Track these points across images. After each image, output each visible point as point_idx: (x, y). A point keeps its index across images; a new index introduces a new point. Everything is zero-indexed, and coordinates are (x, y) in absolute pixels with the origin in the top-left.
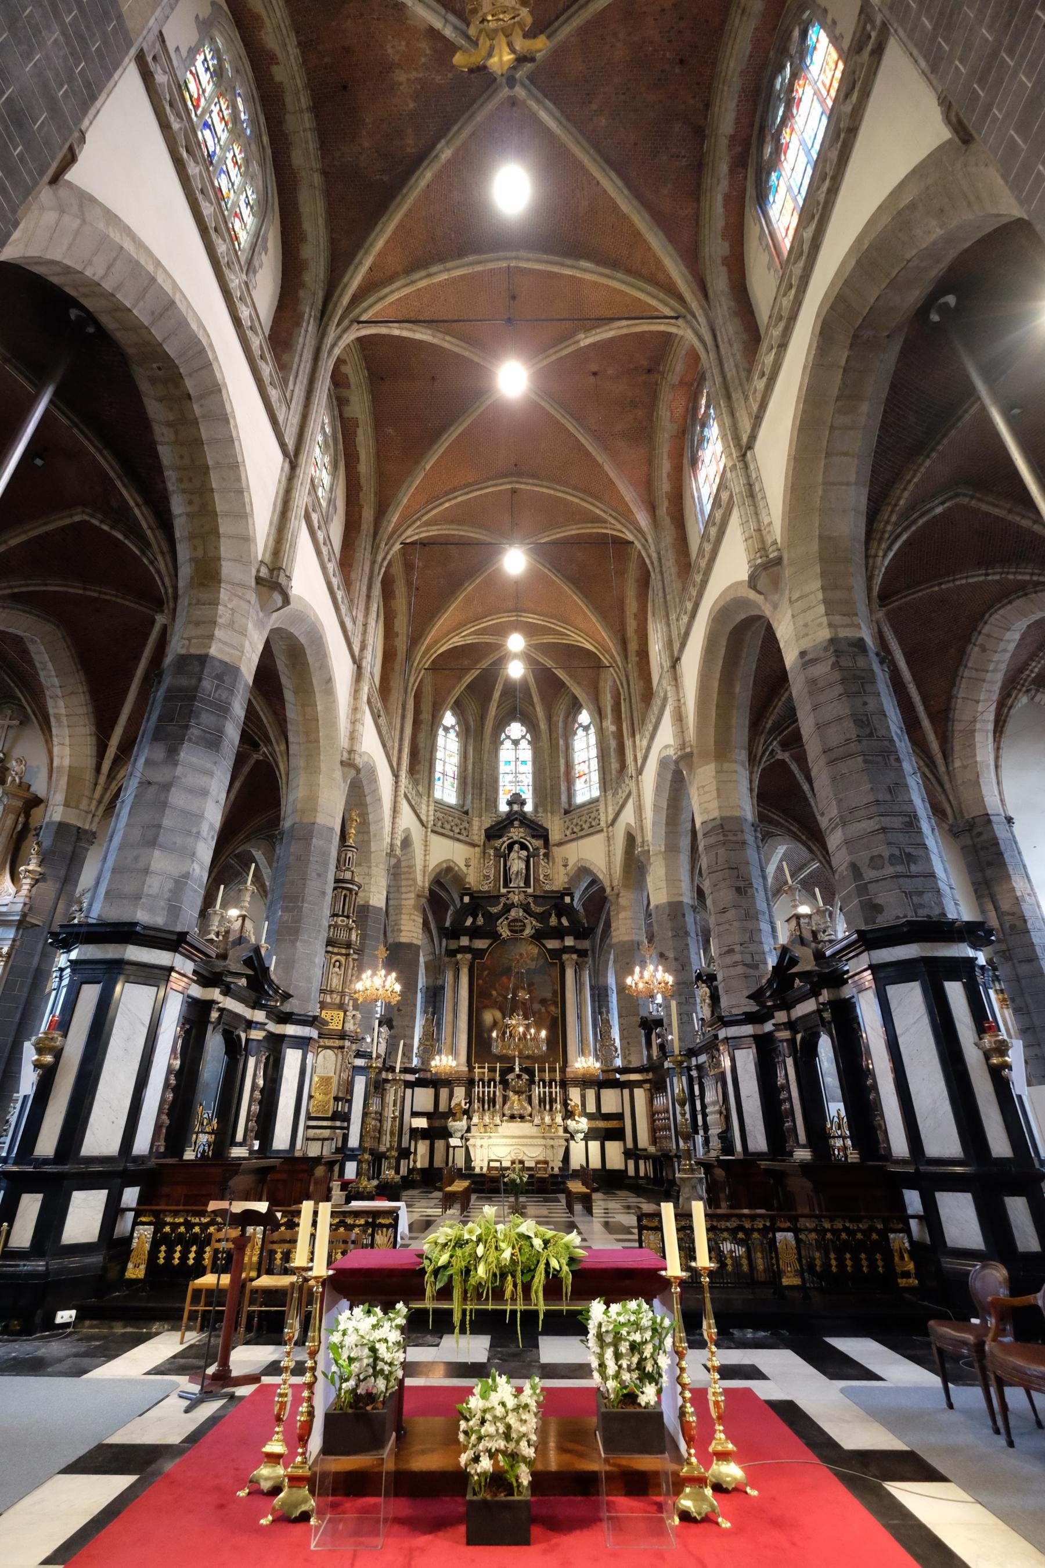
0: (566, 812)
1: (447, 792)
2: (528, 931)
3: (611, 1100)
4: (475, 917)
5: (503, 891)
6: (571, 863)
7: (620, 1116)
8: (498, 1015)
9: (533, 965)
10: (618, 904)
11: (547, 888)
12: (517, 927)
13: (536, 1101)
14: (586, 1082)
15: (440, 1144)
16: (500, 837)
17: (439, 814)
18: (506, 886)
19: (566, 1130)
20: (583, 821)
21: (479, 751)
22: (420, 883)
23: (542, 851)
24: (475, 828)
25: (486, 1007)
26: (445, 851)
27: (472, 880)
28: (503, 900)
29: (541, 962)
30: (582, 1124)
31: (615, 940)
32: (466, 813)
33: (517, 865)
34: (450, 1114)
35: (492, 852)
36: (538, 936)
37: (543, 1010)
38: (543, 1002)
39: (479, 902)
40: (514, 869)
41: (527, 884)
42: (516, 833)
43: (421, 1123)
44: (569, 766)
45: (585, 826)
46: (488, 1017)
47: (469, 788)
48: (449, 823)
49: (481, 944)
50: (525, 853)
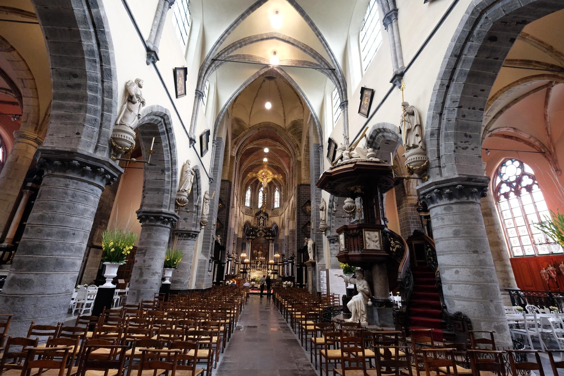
1: (248, 204)
3: (276, 268)
7: (277, 270)
12: (261, 234)
14: (271, 264)
15: (245, 274)
20: (276, 212)
21: (255, 194)
26: (249, 218)
30: (271, 271)
33: (261, 222)
34: (247, 269)
36: (265, 236)
39: (254, 229)
42: (262, 215)
43: (242, 270)
44: (274, 199)
46: (254, 252)
48: (248, 212)
49: (254, 237)
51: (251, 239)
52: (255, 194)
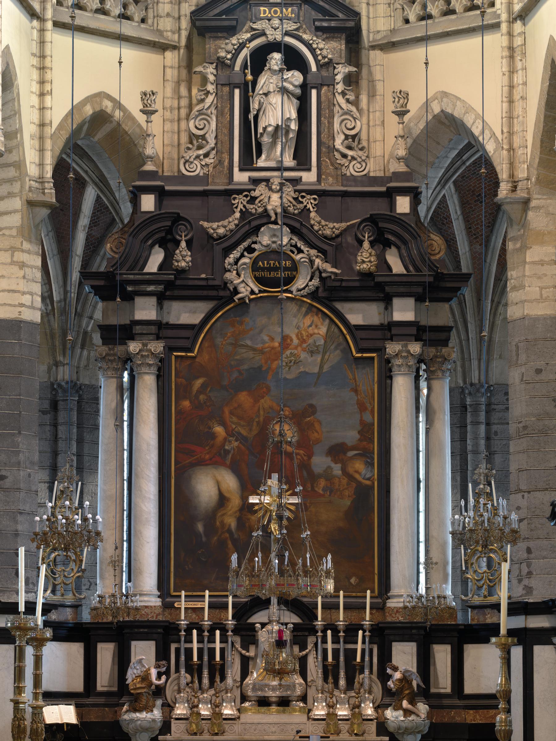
4: (169, 243)
5: (241, 177)
6: (414, 106)
8: (230, 482)
9: (312, 364)
10: (523, 224)
11: (353, 169)
12: (274, 274)
16: (232, 31)
18: (247, 163)
22: (32, 170)
23: (342, 71)
25: (201, 463)
27: (159, 142)
28: (240, 202)
29: (334, 356)
31: (513, 312)
33: (277, 111)
35: (210, 71)
36: (329, 295)
37: (337, 470)
38: (337, 451)
39: (178, 212)
49: (187, 313)
50: (296, 77)
51: (160, 329)
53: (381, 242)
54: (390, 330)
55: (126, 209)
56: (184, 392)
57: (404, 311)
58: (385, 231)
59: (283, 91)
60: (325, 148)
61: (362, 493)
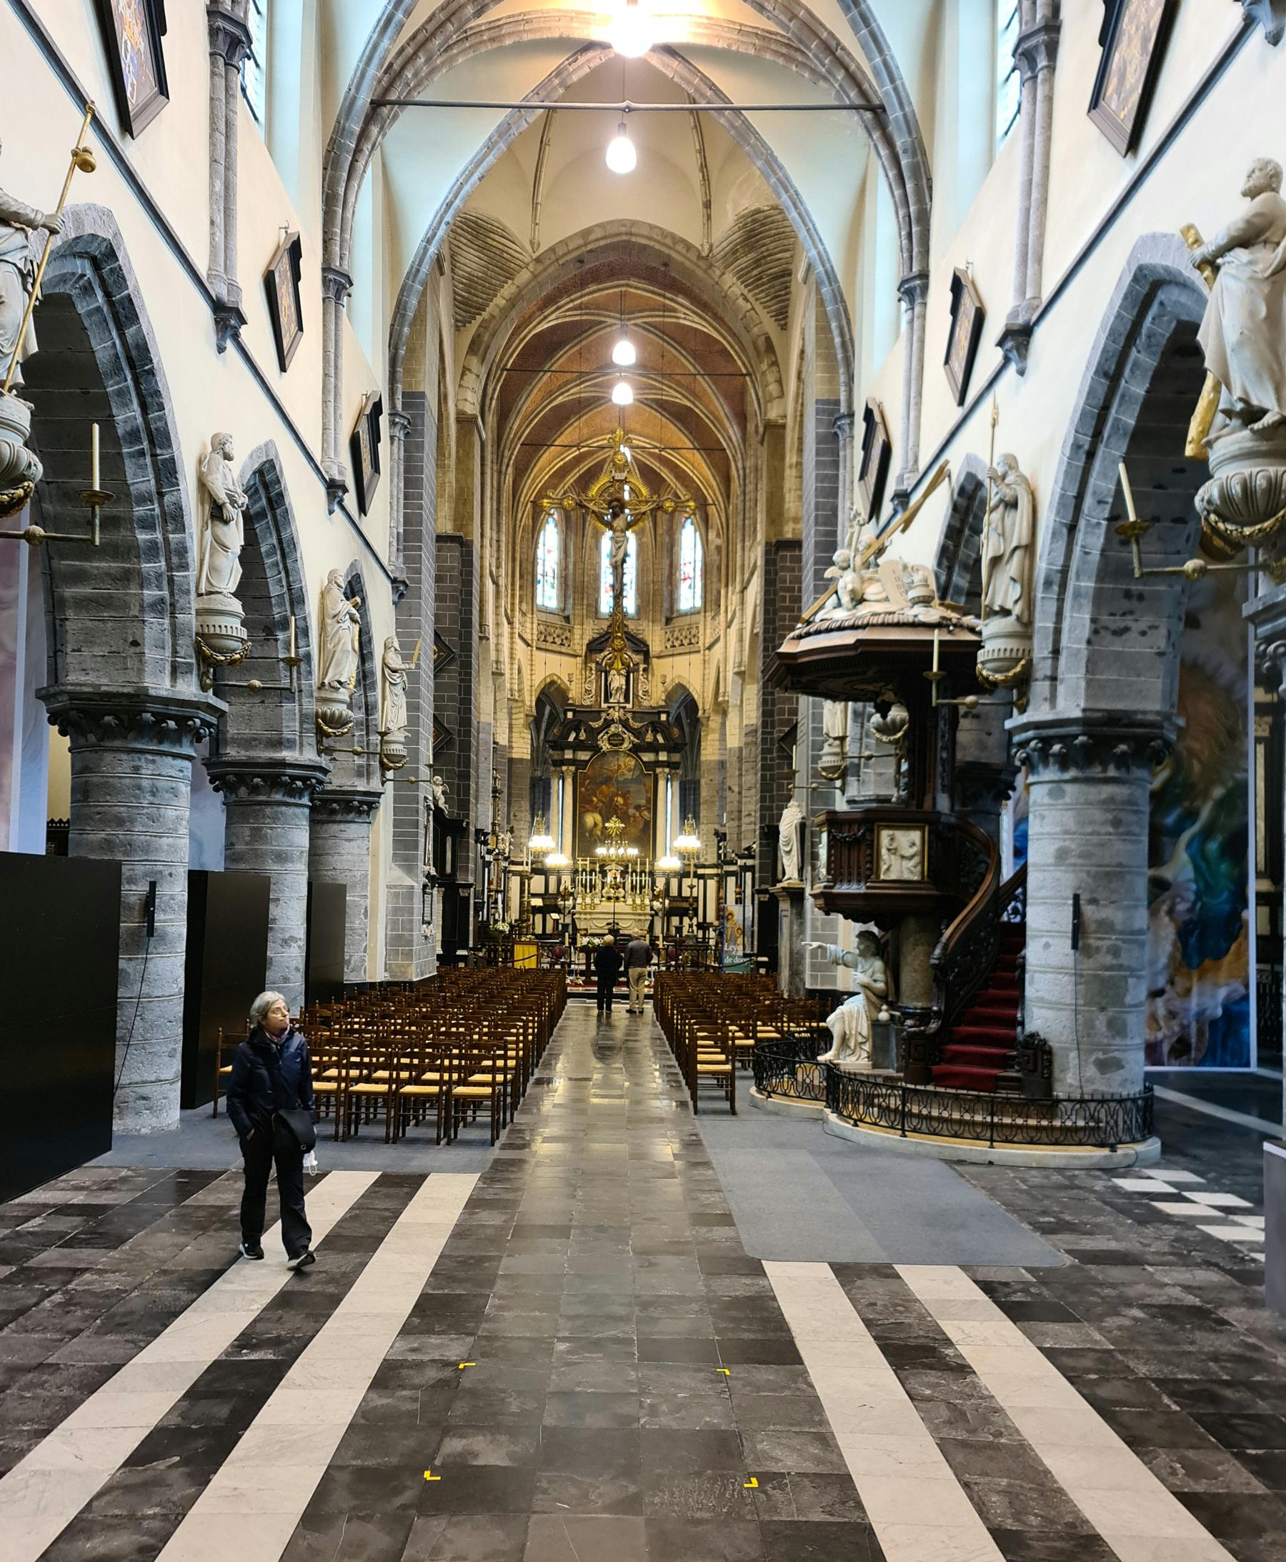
0: (668, 621)
1: (548, 596)
2: (626, 745)
5: (604, 706)
6: (668, 681)
8: (598, 818)
9: (629, 776)
11: (645, 703)
12: (616, 740)
13: (628, 886)
16: (602, 651)
17: (542, 628)
19: (652, 909)
23: (642, 666)
24: (577, 637)
27: (575, 693)
28: (604, 715)
29: (637, 773)
31: (703, 758)
32: (567, 619)
33: (617, 681)
35: (593, 666)
36: (635, 750)
38: (638, 808)
40: (615, 685)
41: (627, 700)
45: (686, 642)
47: (570, 591)
49: (583, 756)
51: (573, 762)
52: (580, 548)
53: (655, 731)
54: (658, 764)
55: (562, 716)
56: (582, 785)
57: (663, 757)
58: (656, 727)
59: (619, 674)
60: (636, 696)
61: (647, 823)
